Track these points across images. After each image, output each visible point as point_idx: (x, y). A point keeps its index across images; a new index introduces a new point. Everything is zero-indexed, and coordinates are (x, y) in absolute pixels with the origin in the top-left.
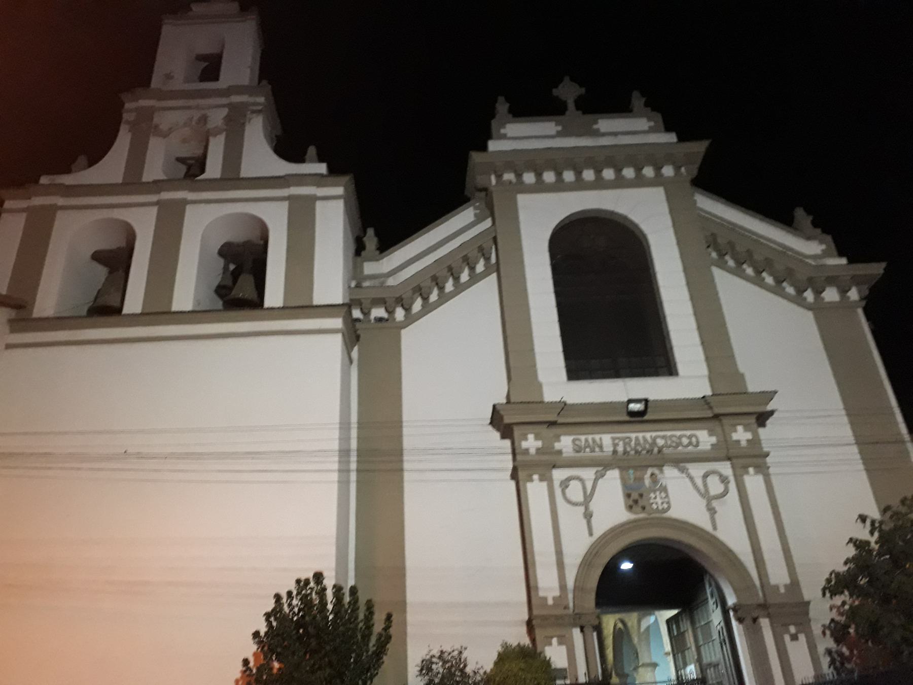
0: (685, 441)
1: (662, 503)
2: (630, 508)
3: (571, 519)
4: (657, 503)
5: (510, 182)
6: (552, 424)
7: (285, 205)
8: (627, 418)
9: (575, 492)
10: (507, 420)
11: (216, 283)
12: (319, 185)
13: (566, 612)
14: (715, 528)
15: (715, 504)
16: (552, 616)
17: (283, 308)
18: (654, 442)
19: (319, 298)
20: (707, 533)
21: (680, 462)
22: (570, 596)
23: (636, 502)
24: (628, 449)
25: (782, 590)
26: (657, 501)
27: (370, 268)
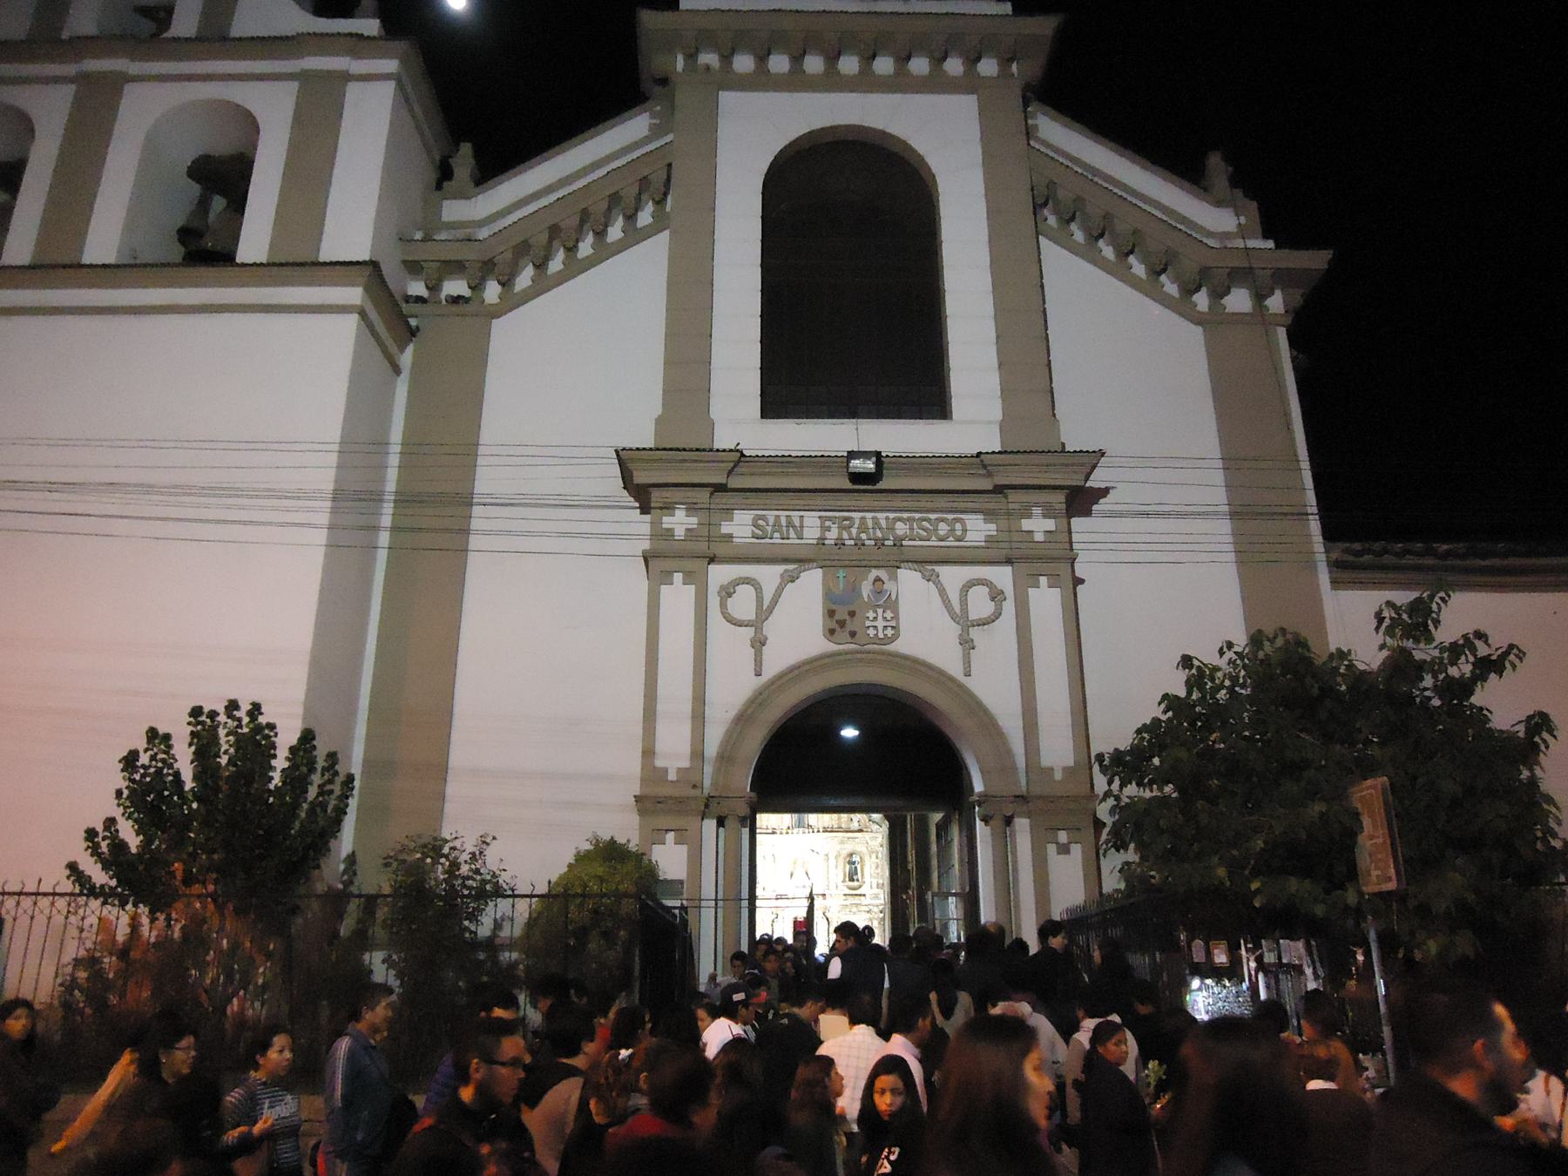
0: (943, 528)
1: (885, 627)
2: (832, 632)
3: (729, 647)
4: (876, 627)
5: (708, 68)
6: (720, 488)
7: (295, 85)
8: (849, 485)
9: (744, 604)
10: (640, 478)
11: (180, 221)
12: (356, 54)
13: (697, 792)
14: (968, 674)
15: (975, 633)
16: (671, 798)
17: (268, 265)
18: (891, 529)
19: (329, 251)
20: (952, 679)
21: (926, 562)
22: (708, 770)
23: (842, 624)
24: (845, 535)
25: (1058, 776)
26: (877, 623)
27: (454, 210)
